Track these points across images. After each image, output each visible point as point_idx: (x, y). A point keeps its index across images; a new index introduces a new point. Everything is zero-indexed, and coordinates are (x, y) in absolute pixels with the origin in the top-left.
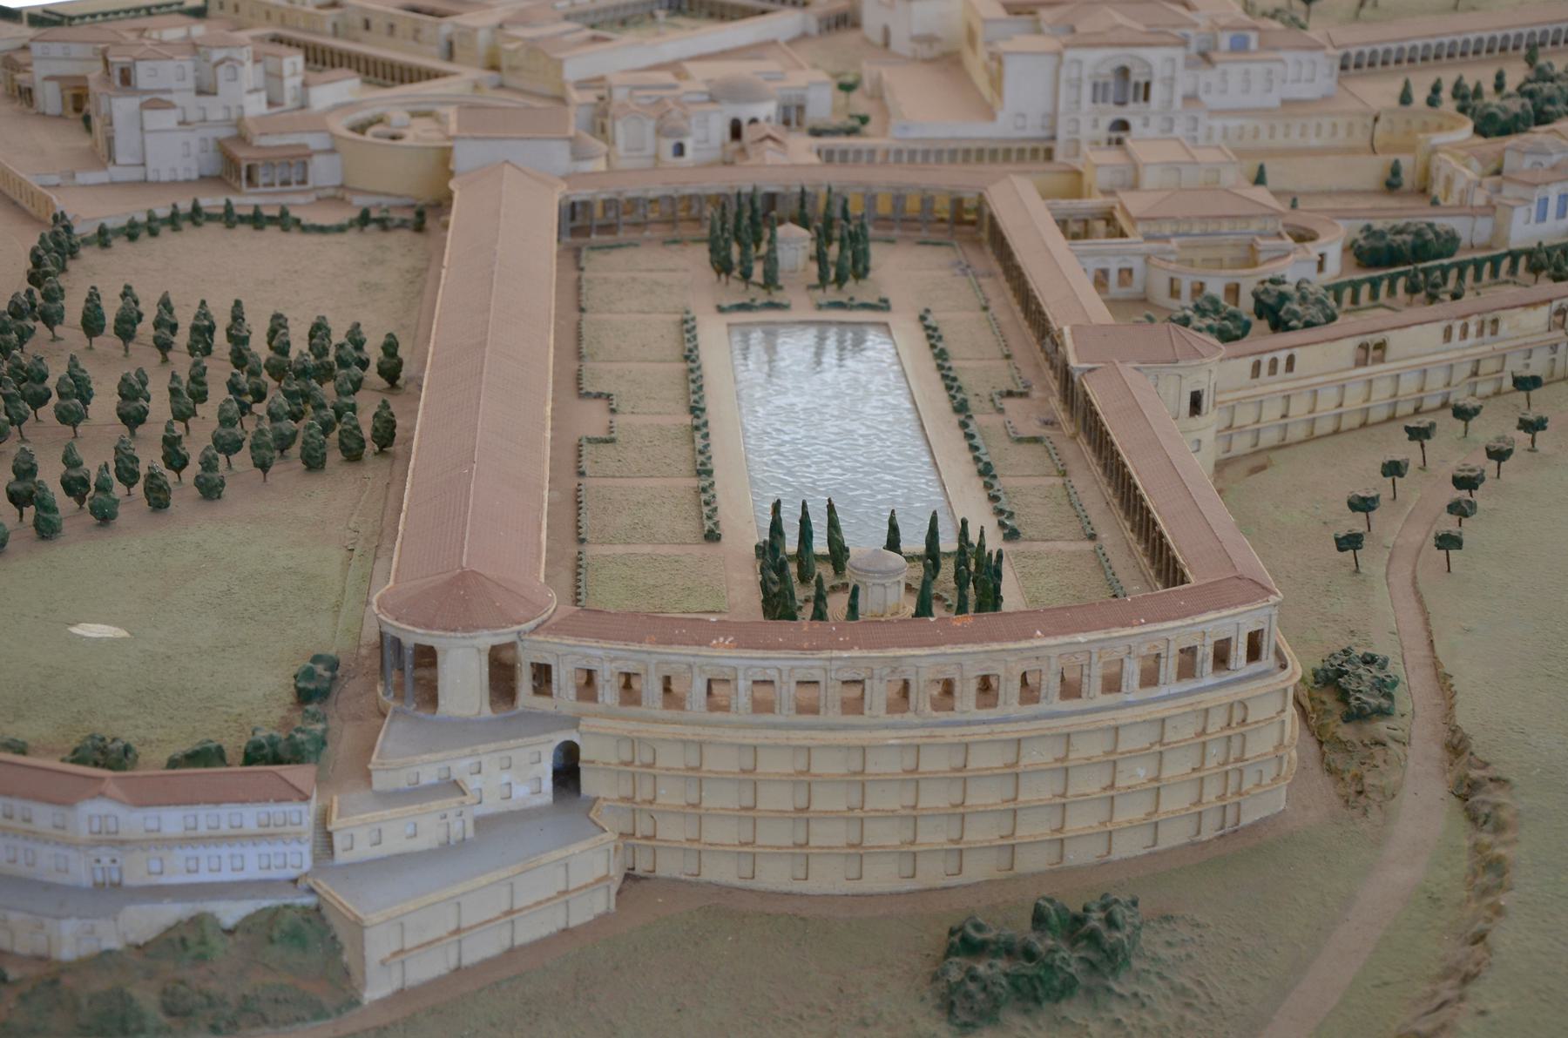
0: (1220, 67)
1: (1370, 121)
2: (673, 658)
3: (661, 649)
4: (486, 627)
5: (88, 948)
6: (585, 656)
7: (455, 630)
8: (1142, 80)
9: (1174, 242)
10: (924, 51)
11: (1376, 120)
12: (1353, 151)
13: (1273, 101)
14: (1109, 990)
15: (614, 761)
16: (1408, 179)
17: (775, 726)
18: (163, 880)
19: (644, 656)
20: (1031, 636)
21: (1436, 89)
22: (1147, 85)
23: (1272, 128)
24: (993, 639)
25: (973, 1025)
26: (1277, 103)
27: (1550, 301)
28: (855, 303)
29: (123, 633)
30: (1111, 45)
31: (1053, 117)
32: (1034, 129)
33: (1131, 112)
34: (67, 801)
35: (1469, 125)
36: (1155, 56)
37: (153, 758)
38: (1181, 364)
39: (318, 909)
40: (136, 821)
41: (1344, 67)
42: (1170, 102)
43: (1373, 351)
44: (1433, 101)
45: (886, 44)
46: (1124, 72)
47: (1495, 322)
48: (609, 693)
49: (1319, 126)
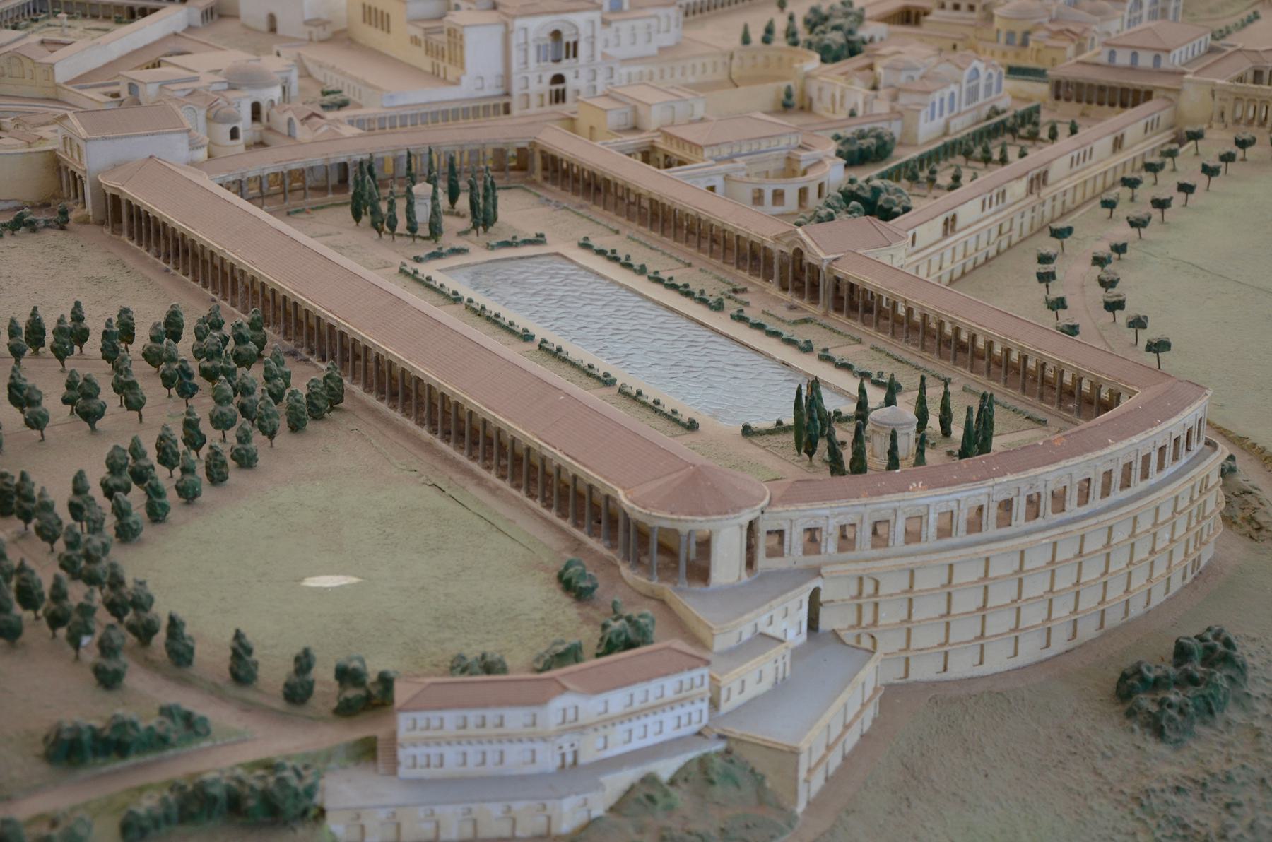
0: (614, 25)
1: (727, 59)
2: (884, 506)
3: (875, 500)
4: (747, 507)
5: (580, 818)
6: (878, 511)
7: (726, 513)
8: (571, 40)
9: (741, 162)
10: (319, 33)
11: (731, 58)
12: (716, 85)
13: (652, 49)
14: (1248, 695)
15: (847, 597)
16: (795, 99)
17: (924, 553)
18: (608, 754)
19: (861, 509)
20: (1108, 445)
21: (769, 30)
22: (575, 44)
23: (662, 71)
24: (1088, 451)
25: (1181, 741)
26: (655, 51)
27: (1027, 173)
28: (519, 240)
29: (354, 580)
30: (548, 13)
31: (506, 77)
32: (491, 88)
33: (564, 68)
34: (542, 701)
35: (817, 57)
36: (580, 19)
37: (518, 659)
38: (894, 245)
39: (728, 752)
40: (591, 707)
41: (686, 14)
42: (593, 56)
43: (950, 225)
44: (766, 40)
45: (273, 30)
46: (556, 35)
47: (1004, 192)
48: (830, 545)
49: (694, 66)
